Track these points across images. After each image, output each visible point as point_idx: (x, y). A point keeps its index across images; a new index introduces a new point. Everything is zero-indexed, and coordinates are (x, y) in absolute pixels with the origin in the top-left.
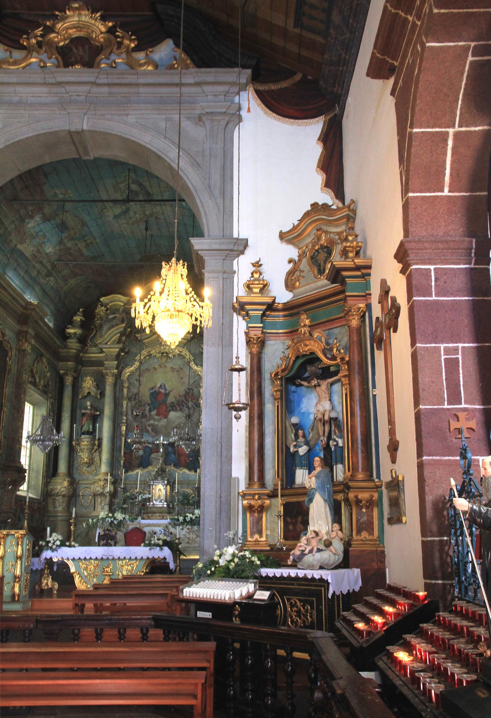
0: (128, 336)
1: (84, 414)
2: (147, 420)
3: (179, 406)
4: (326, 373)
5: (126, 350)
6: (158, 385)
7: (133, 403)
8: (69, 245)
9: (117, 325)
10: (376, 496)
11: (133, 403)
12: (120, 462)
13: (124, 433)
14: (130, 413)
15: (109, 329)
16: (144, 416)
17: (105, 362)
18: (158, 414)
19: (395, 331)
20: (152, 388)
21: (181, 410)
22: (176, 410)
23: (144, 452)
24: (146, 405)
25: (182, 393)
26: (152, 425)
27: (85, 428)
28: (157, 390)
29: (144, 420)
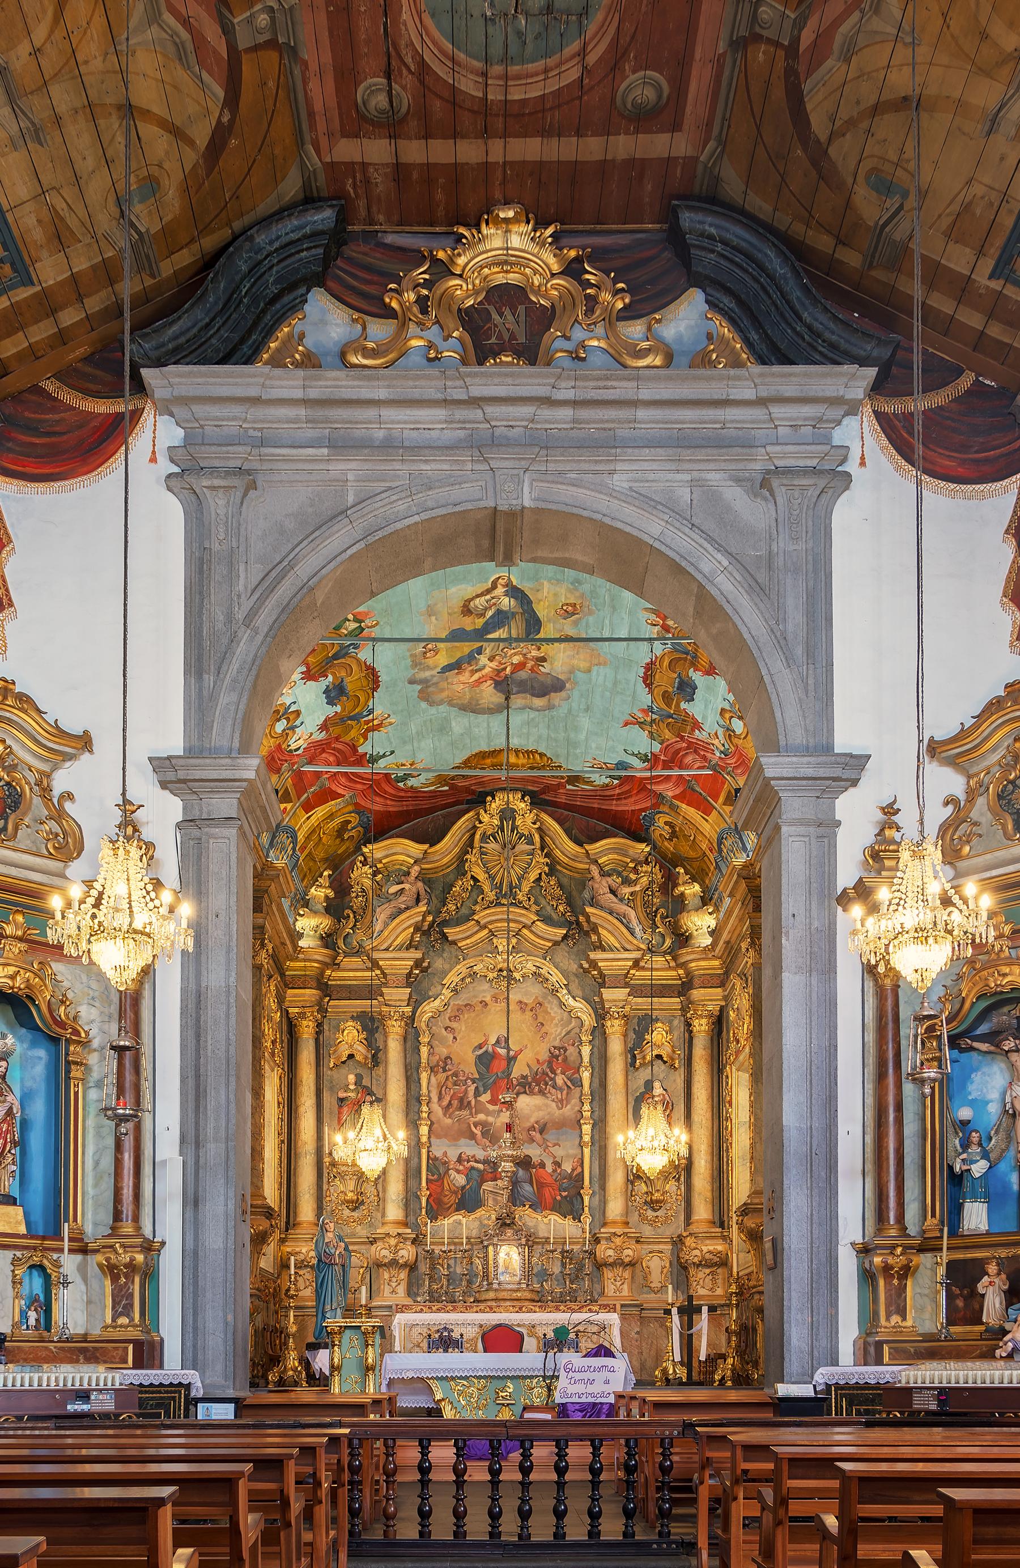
0: (426, 933)
2: (471, 1114)
3: (538, 1084)
5: (425, 964)
6: (493, 1040)
7: (442, 1076)
9: (407, 908)
11: (442, 1076)
12: (418, 1198)
13: (424, 1139)
14: (435, 1098)
15: (393, 917)
16: (463, 1104)
17: (384, 990)
18: (494, 1101)
20: (480, 1046)
21: (541, 1092)
22: (532, 1093)
23: (468, 1180)
24: (469, 1082)
25: (544, 1056)
26: (484, 1124)
28: (490, 1049)
29: (465, 1113)
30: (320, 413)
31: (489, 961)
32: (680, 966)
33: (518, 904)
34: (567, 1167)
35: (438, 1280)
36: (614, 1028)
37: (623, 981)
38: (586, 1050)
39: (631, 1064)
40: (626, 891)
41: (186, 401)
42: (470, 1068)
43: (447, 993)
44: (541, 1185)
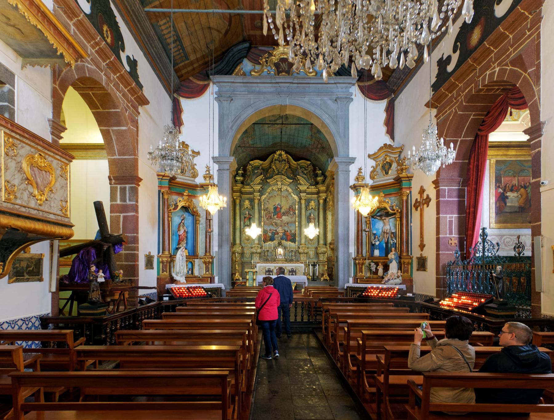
1: (245, 217)
4: (388, 215)
8: (245, 139)
10: (410, 261)
16: (271, 218)
19: (428, 206)
26: (275, 222)
27: (246, 223)
30: (246, 85)
31: (276, 186)
32: (318, 188)
33: (283, 175)
34: (293, 232)
35: (267, 257)
36: (303, 202)
37: (305, 192)
38: (297, 206)
39: (306, 209)
40: (305, 172)
41: (219, 82)
42: (272, 210)
43: (267, 194)
44: (287, 236)
